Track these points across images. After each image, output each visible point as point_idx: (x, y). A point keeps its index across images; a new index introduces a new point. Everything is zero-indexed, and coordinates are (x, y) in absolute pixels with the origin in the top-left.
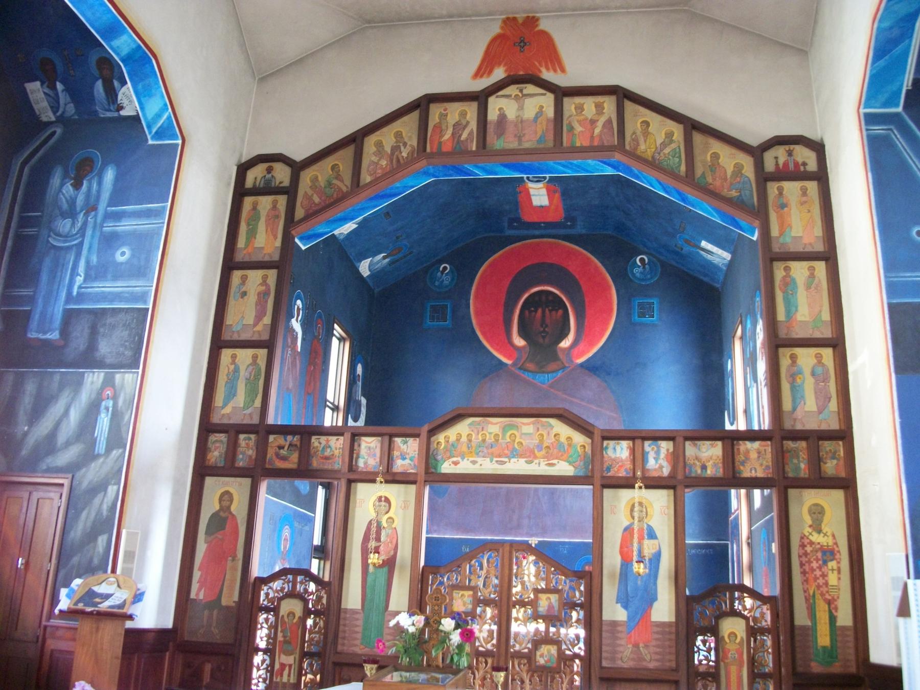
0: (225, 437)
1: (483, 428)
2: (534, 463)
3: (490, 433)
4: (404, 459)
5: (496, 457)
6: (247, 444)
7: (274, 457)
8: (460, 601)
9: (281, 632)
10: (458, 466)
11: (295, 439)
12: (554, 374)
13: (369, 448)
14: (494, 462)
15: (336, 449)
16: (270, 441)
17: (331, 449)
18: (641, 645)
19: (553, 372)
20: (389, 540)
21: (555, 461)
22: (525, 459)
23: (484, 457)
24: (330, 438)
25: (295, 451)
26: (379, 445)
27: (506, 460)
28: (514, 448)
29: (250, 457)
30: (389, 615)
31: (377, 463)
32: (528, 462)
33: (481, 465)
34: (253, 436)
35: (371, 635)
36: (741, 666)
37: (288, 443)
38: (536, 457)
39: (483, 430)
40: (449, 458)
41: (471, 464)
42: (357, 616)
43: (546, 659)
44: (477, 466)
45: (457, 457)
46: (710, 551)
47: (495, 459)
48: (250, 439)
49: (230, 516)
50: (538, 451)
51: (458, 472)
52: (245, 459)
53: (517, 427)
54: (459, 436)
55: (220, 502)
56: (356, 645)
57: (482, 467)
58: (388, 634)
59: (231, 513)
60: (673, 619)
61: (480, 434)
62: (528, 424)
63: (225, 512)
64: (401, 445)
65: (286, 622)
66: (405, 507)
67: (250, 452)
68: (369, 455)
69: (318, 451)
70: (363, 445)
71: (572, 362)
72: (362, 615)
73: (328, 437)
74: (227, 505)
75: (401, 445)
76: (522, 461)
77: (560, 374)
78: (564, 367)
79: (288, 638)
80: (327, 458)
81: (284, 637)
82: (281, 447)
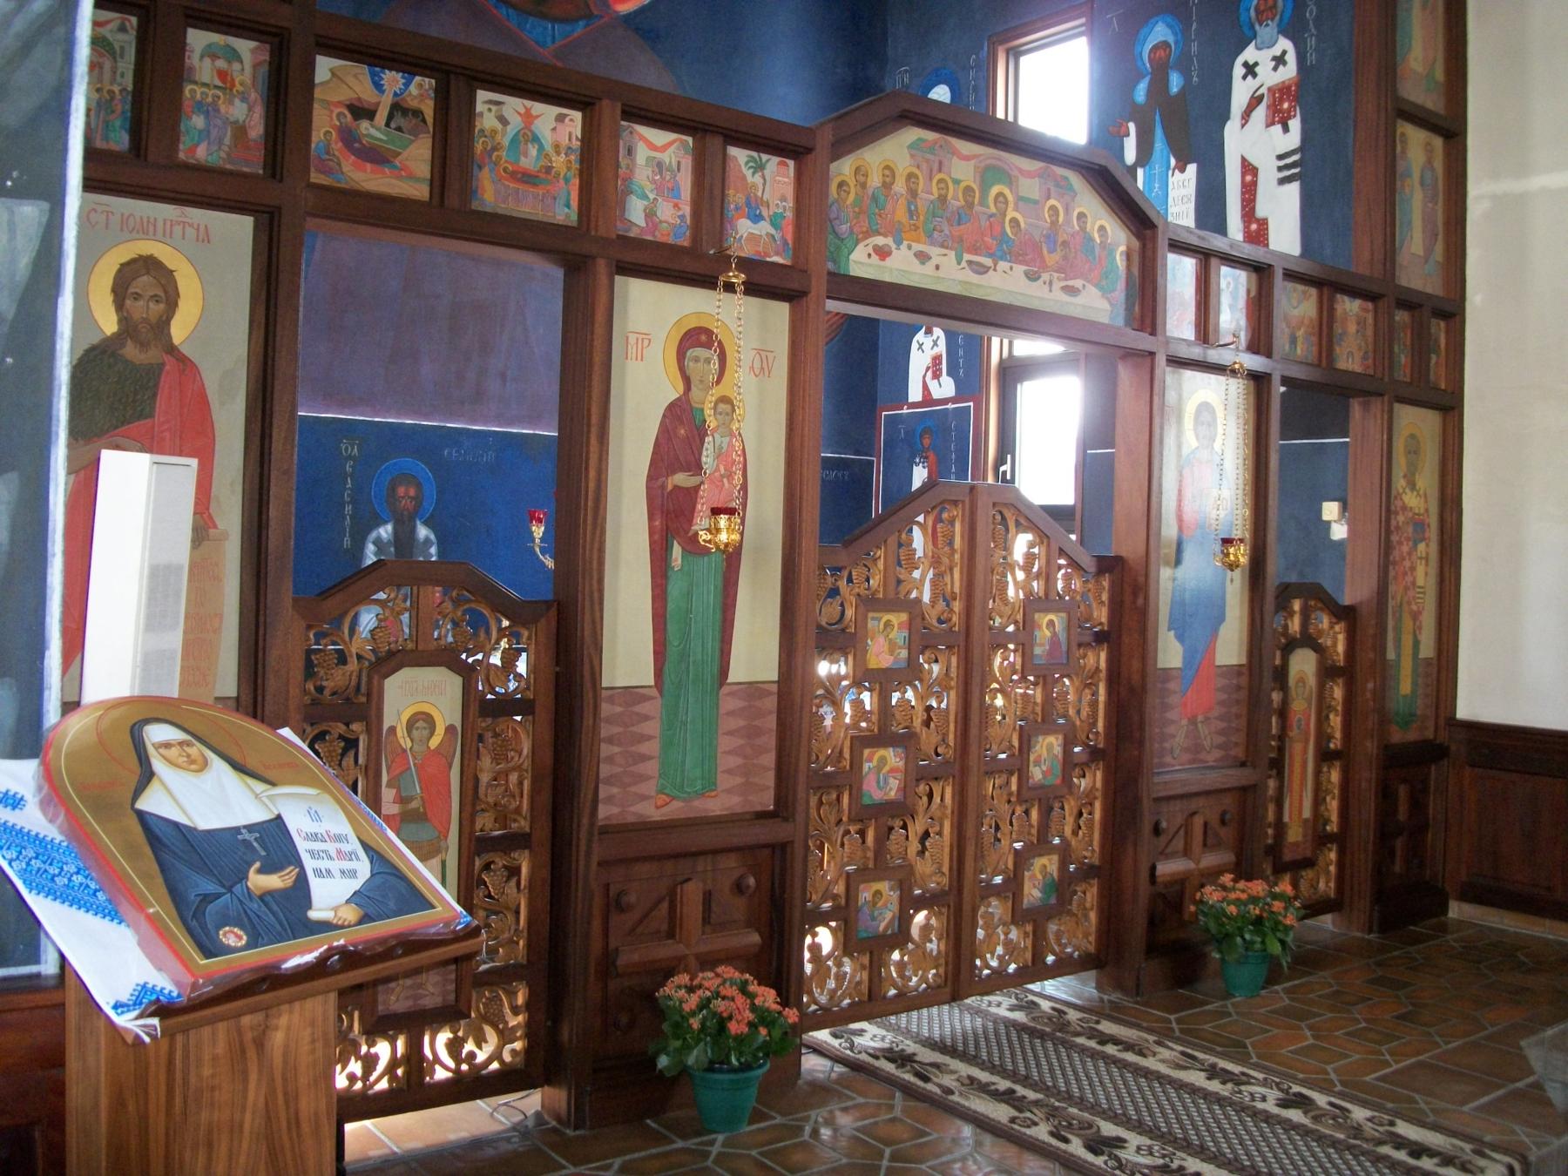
0: (122, 29)
1: (940, 163)
2: (1040, 282)
3: (957, 182)
4: (757, 218)
5: (969, 252)
6: (222, 75)
7: (337, 146)
8: (881, 639)
9: (389, 785)
10: (889, 262)
11: (413, 89)
12: (568, 28)
13: (660, 165)
14: (964, 264)
15: (558, 153)
16: (318, 80)
17: (541, 147)
18: (1200, 718)
19: (564, 20)
20: (723, 471)
21: (1078, 283)
22: (1025, 268)
23: (942, 246)
24: (538, 107)
25: (415, 133)
26: (688, 163)
27: (987, 261)
28: (1004, 233)
29: (240, 130)
30: (730, 694)
31: (682, 217)
32: (1032, 277)
33: (937, 267)
34: (245, 46)
35: (683, 762)
36: (1307, 741)
37: (386, 101)
38: (1044, 267)
39: (940, 170)
40: (868, 234)
41: (916, 261)
42: (644, 708)
43: (1044, 768)
44: (930, 265)
45: (885, 236)
46: (843, 476)
47: (967, 257)
48: (234, 56)
49: (170, 364)
50: (1050, 252)
51: (887, 278)
52: (214, 132)
53: (1010, 181)
54: (889, 172)
55: (119, 305)
56: (644, 798)
57: (940, 273)
58: (729, 753)
59: (172, 349)
60: (1244, 661)
61: (935, 181)
62: (1030, 175)
63: (144, 345)
64: (748, 173)
65: (404, 751)
66: (762, 368)
67: (238, 111)
68: (659, 189)
69: (495, 149)
70: (642, 153)
71: (608, 6)
72: (659, 699)
73: (528, 103)
74: (153, 319)
75: (748, 173)
76: (1020, 269)
77: (580, 28)
78: (589, 16)
79: (414, 804)
80: (526, 178)
81: (401, 800)
82: (361, 111)
